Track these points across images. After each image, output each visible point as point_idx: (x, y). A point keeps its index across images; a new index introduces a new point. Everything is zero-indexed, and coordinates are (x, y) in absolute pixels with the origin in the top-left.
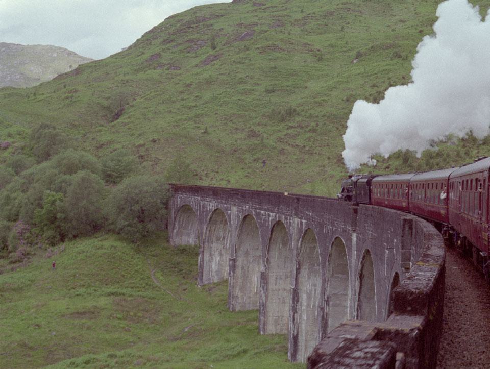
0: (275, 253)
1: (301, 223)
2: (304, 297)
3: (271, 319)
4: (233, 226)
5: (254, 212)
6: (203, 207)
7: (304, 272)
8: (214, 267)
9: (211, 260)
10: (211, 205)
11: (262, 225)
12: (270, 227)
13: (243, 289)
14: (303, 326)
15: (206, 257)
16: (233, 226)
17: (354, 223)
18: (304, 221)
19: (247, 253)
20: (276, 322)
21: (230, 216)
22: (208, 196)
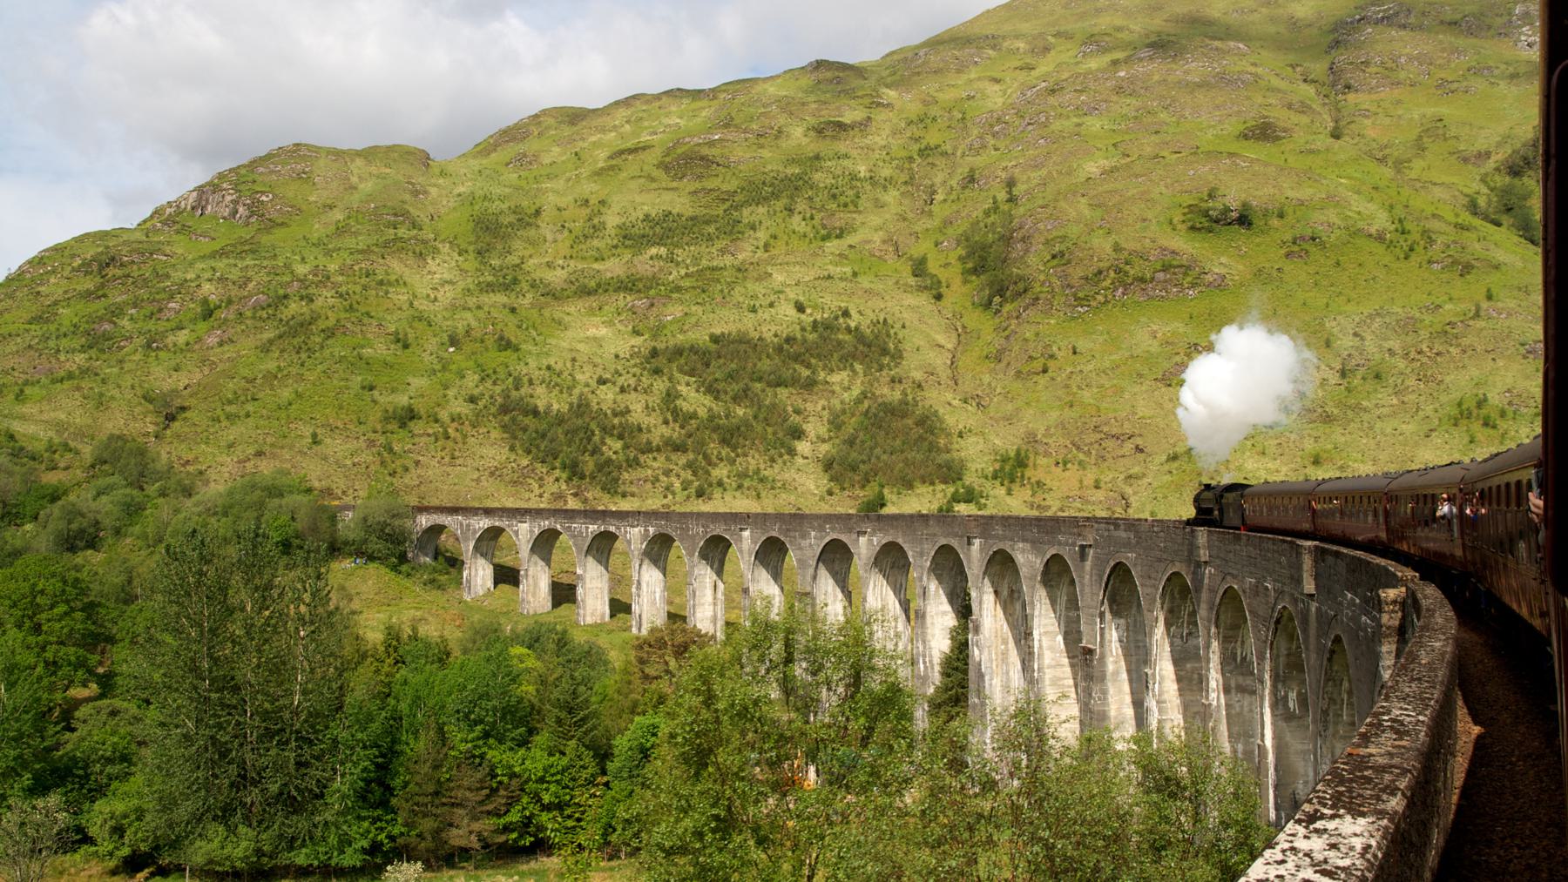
1: (647, 531)
2: (644, 586)
3: (589, 612)
4: (523, 541)
5: (558, 527)
6: (468, 525)
7: (644, 567)
8: (479, 581)
9: (476, 576)
10: (484, 523)
11: (574, 537)
12: (590, 537)
13: (534, 595)
16: (523, 541)
21: (517, 533)
22: (476, 514)
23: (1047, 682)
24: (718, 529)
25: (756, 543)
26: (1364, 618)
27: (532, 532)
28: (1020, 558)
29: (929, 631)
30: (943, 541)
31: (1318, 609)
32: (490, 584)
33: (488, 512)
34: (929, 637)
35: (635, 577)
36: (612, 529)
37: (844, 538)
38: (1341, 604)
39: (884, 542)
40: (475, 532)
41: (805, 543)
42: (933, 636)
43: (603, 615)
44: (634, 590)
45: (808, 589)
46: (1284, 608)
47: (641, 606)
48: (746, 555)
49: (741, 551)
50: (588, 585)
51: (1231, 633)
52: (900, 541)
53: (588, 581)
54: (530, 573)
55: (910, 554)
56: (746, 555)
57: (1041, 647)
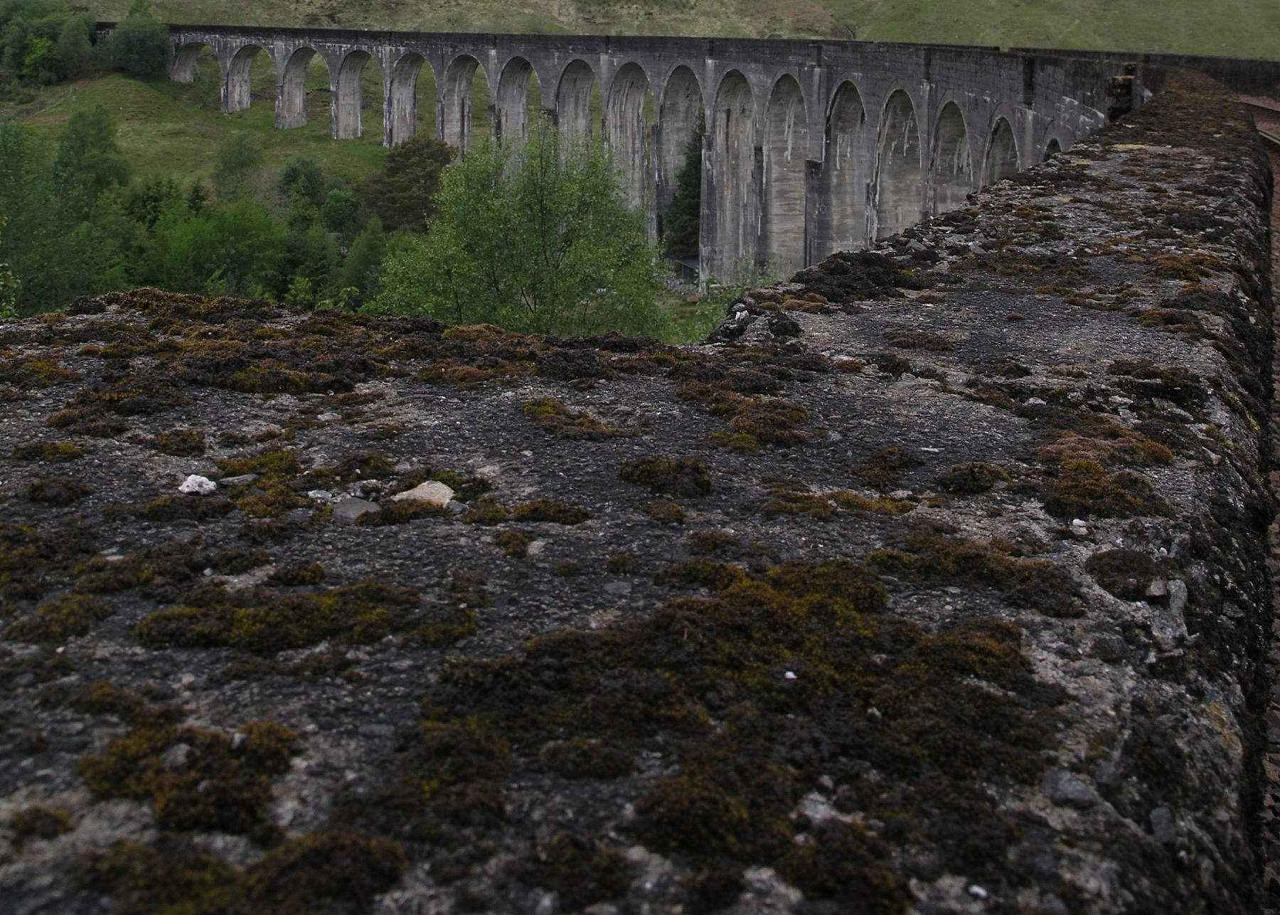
0: (343, 76)
2: (395, 102)
3: (341, 128)
6: (225, 44)
7: (395, 85)
8: (237, 97)
9: (233, 92)
10: (238, 42)
13: (289, 110)
14: (395, 123)
15: (230, 88)
17: (495, 45)
18: (402, 49)
19: (291, 81)
20: (345, 130)
21: (272, 51)
23: (774, 195)
24: (467, 49)
25: (502, 63)
26: (1082, 118)
27: (287, 50)
28: (752, 78)
29: (664, 147)
30: (681, 62)
31: (1035, 117)
32: (247, 100)
33: (245, 31)
34: (664, 153)
35: (386, 96)
36: (364, 48)
37: (585, 58)
38: (1058, 109)
39: (624, 62)
40: (232, 49)
41: (548, 63)
42: (669, 151)
43: (355, 130)
44: (385, 106)
45: (551, 107)
46: (1002, 119)
47: (391, 122)
48: (493, 75)
49: (487, 70)
50: (341, 102)
51: (949, 146)
52: (639, 62)
53: (341, 98)
54: (286, 89)
55: (648, 74)
56: (493, 75)
57: (769, 162)
